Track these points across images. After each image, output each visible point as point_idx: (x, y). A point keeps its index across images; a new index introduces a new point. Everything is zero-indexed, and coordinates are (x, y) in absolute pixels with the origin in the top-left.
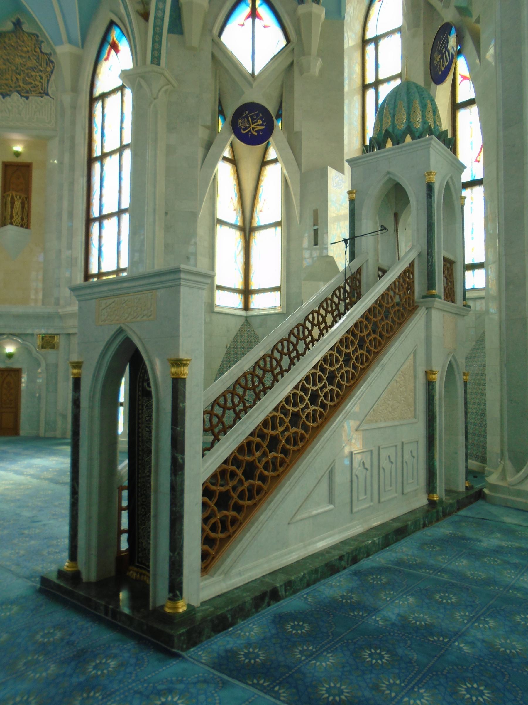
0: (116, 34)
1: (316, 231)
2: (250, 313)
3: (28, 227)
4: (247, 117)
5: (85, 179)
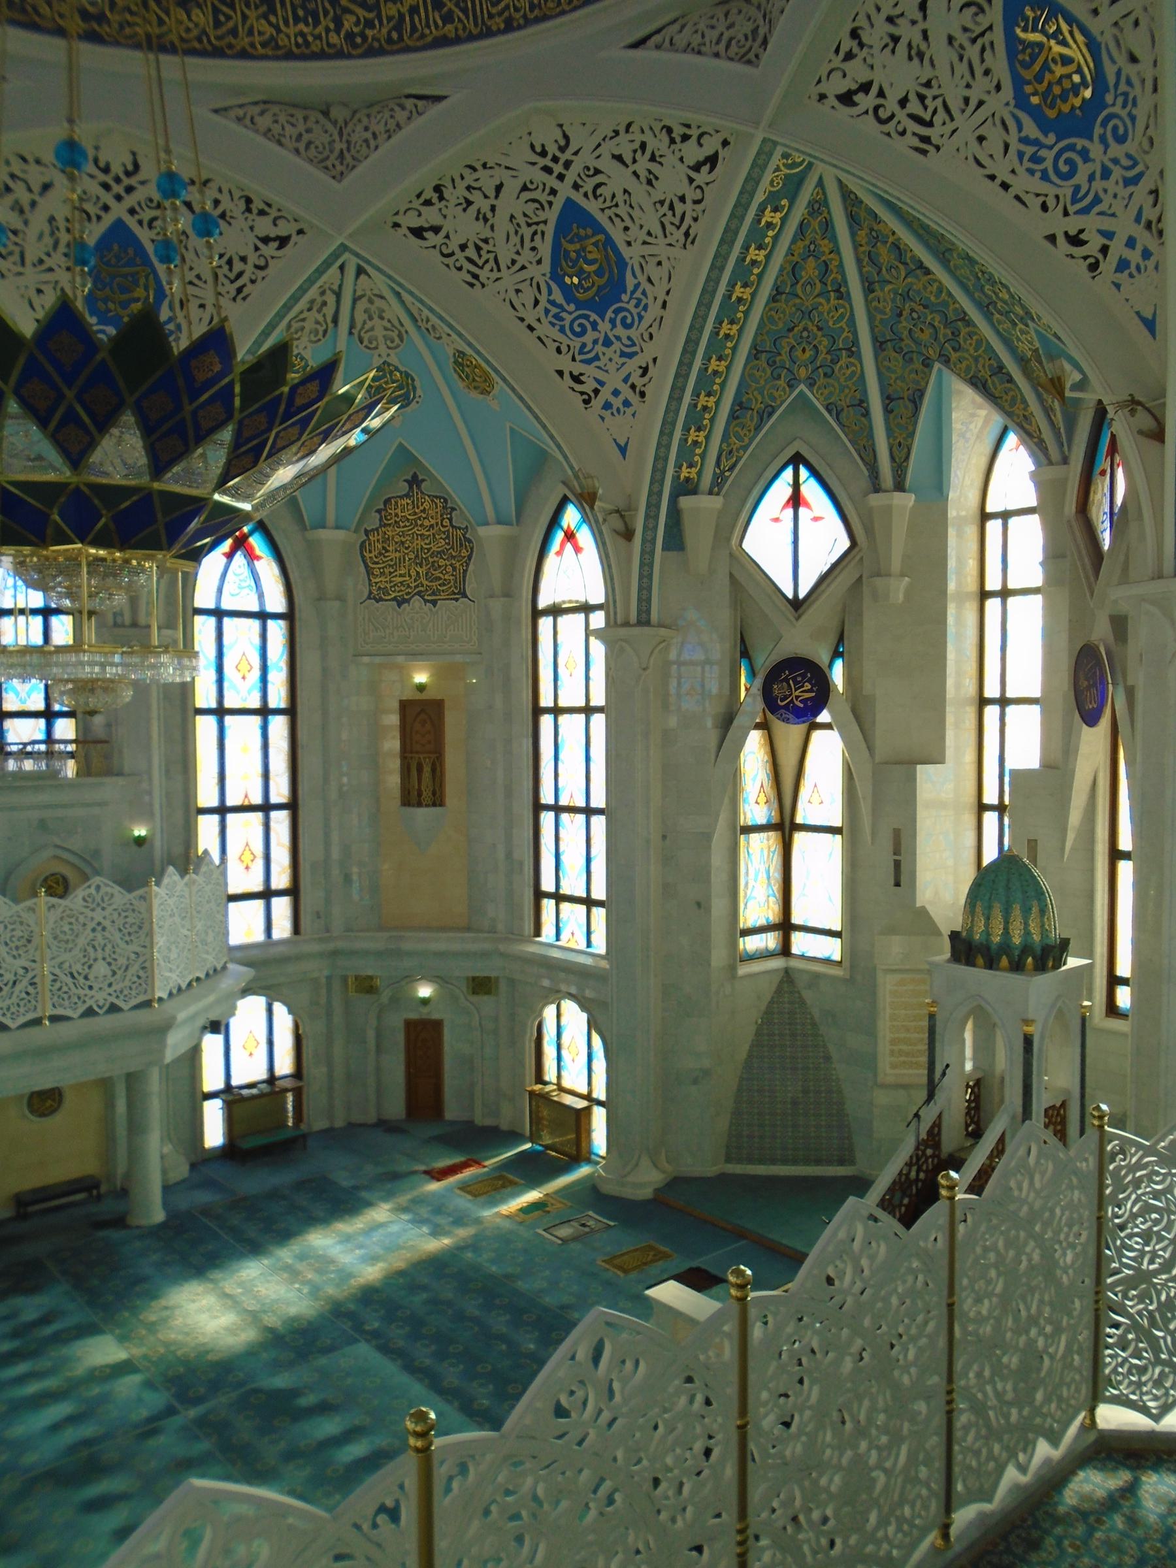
0: (571, 516)
1: (897, 865)
2: (793, 963)
3: (442, 804)
4: (786, 680)
5: (531, 741)
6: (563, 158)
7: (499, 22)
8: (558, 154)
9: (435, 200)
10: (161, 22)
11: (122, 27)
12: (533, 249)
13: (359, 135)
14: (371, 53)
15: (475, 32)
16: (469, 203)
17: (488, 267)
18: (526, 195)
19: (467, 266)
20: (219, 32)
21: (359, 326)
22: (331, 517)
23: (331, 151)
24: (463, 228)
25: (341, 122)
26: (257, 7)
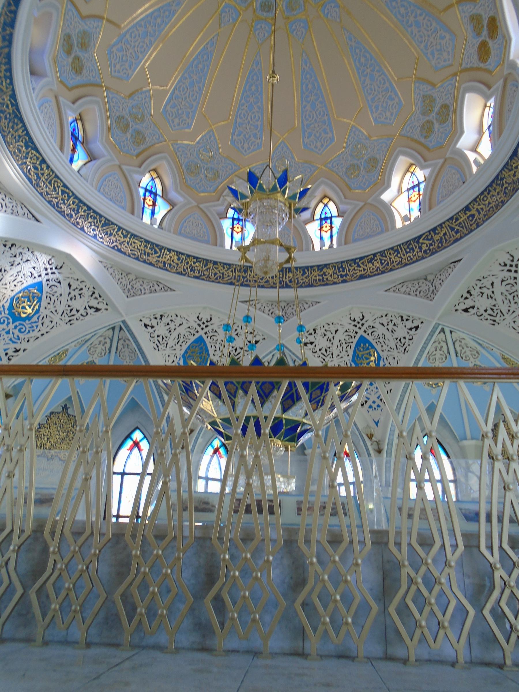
6: (514, 264)
7: (475, 226)
8: (512, 263)
9: (468, 295)
10: (364, 270)
11: (353, 275)
12: (516, 303)
13: (437, 282)
14: (433, 253)
15: (467, 232)
16: (482, 293)
17: (498, 316)
18: (504, 283)
19: (490, 318)
20: (383, 266)
21: (459, 352)
22: (468, 435)
23: (429, 291)
24: (483, 303)
25: (432, 280)
26: (393, 254)
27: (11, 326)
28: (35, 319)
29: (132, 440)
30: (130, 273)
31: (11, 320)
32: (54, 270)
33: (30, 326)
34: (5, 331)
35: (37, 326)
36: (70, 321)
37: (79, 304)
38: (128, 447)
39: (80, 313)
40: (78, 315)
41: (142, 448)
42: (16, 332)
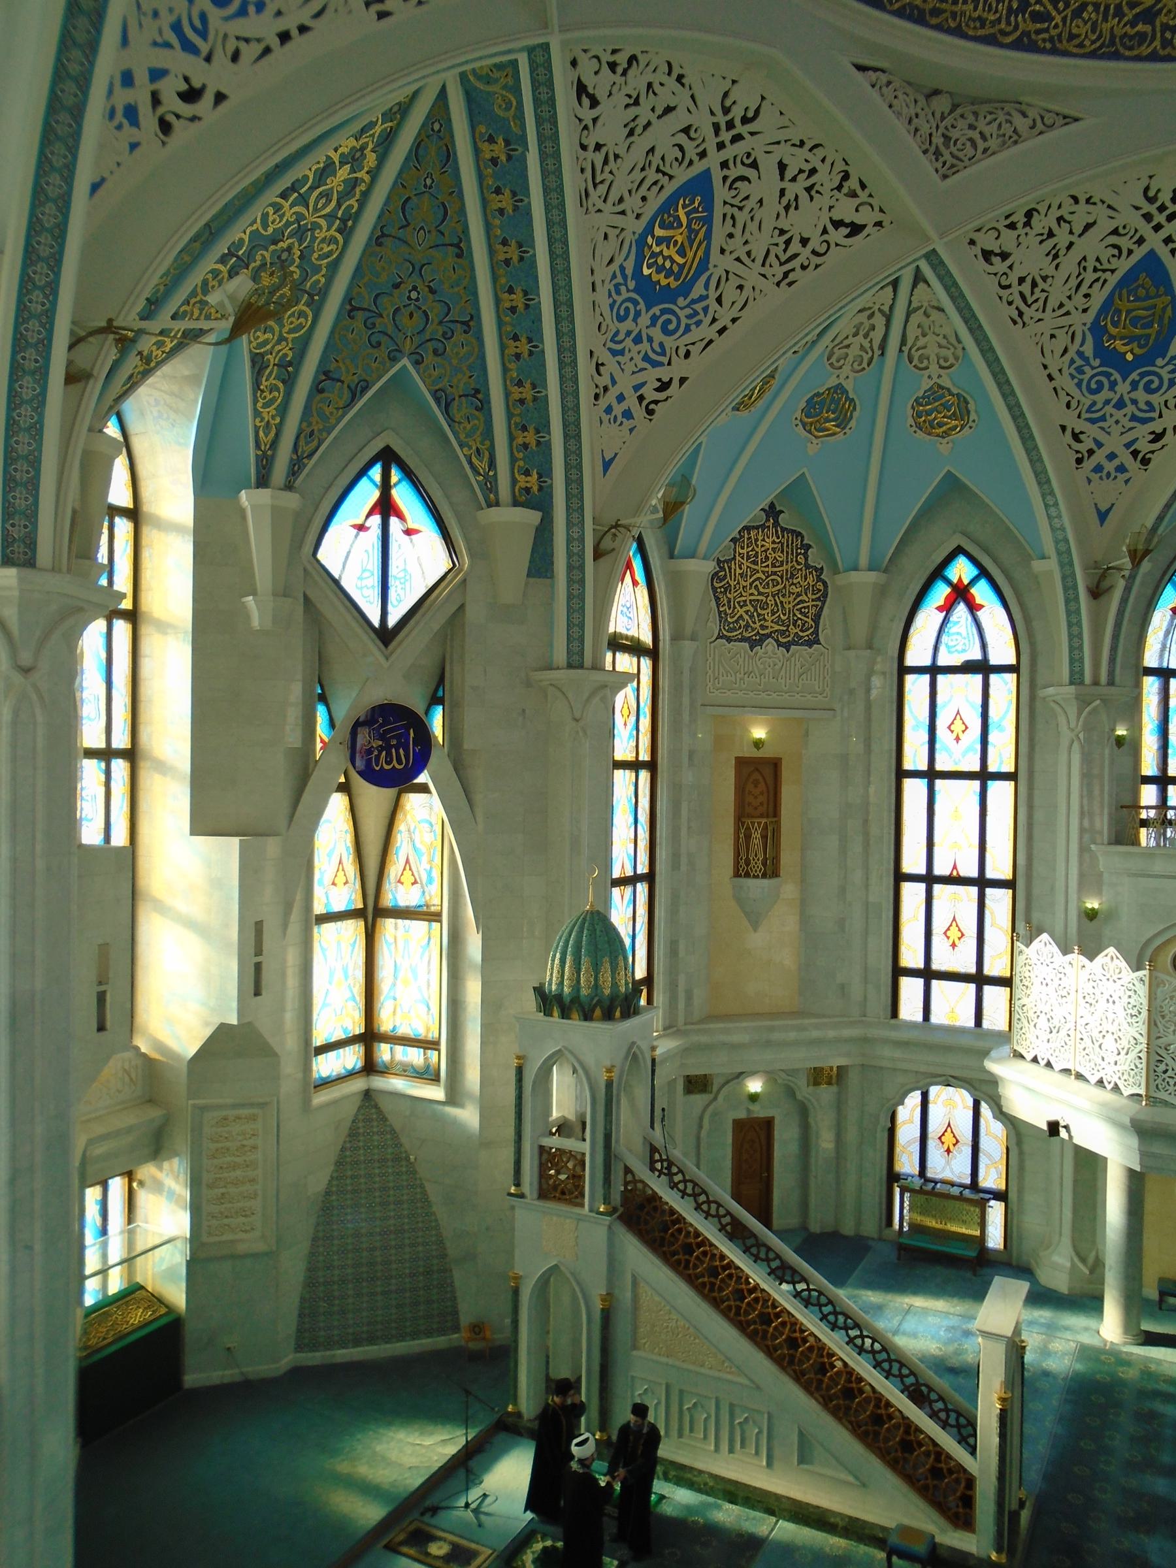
27: (645, 320)
28: (698, 290)
29: (948, 582)
30: (936, 92)
31: (642, 306)
32: (740, 129)
33: (689, 311)
34: (632, 336)
35: (706, 309)
36: (786, 275)
37: (808, 220)
38: (941, 602)
39: (810, 247)
40: (806, 252)
41: (978, 601)
42: (656, 333)
